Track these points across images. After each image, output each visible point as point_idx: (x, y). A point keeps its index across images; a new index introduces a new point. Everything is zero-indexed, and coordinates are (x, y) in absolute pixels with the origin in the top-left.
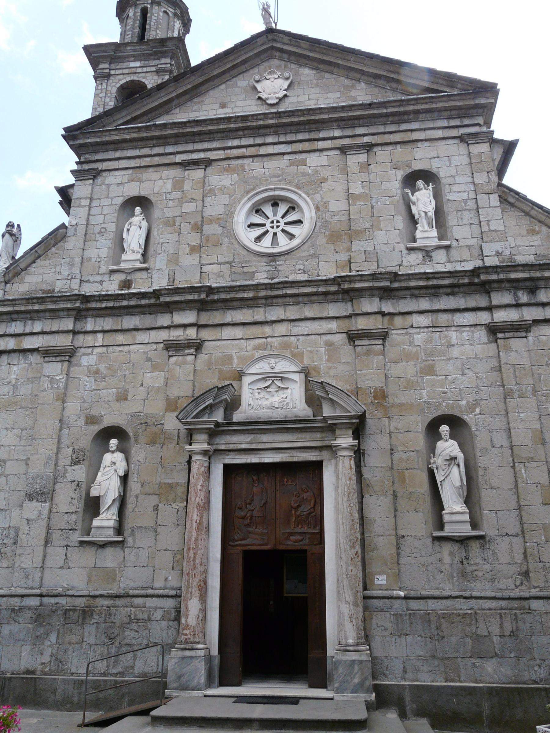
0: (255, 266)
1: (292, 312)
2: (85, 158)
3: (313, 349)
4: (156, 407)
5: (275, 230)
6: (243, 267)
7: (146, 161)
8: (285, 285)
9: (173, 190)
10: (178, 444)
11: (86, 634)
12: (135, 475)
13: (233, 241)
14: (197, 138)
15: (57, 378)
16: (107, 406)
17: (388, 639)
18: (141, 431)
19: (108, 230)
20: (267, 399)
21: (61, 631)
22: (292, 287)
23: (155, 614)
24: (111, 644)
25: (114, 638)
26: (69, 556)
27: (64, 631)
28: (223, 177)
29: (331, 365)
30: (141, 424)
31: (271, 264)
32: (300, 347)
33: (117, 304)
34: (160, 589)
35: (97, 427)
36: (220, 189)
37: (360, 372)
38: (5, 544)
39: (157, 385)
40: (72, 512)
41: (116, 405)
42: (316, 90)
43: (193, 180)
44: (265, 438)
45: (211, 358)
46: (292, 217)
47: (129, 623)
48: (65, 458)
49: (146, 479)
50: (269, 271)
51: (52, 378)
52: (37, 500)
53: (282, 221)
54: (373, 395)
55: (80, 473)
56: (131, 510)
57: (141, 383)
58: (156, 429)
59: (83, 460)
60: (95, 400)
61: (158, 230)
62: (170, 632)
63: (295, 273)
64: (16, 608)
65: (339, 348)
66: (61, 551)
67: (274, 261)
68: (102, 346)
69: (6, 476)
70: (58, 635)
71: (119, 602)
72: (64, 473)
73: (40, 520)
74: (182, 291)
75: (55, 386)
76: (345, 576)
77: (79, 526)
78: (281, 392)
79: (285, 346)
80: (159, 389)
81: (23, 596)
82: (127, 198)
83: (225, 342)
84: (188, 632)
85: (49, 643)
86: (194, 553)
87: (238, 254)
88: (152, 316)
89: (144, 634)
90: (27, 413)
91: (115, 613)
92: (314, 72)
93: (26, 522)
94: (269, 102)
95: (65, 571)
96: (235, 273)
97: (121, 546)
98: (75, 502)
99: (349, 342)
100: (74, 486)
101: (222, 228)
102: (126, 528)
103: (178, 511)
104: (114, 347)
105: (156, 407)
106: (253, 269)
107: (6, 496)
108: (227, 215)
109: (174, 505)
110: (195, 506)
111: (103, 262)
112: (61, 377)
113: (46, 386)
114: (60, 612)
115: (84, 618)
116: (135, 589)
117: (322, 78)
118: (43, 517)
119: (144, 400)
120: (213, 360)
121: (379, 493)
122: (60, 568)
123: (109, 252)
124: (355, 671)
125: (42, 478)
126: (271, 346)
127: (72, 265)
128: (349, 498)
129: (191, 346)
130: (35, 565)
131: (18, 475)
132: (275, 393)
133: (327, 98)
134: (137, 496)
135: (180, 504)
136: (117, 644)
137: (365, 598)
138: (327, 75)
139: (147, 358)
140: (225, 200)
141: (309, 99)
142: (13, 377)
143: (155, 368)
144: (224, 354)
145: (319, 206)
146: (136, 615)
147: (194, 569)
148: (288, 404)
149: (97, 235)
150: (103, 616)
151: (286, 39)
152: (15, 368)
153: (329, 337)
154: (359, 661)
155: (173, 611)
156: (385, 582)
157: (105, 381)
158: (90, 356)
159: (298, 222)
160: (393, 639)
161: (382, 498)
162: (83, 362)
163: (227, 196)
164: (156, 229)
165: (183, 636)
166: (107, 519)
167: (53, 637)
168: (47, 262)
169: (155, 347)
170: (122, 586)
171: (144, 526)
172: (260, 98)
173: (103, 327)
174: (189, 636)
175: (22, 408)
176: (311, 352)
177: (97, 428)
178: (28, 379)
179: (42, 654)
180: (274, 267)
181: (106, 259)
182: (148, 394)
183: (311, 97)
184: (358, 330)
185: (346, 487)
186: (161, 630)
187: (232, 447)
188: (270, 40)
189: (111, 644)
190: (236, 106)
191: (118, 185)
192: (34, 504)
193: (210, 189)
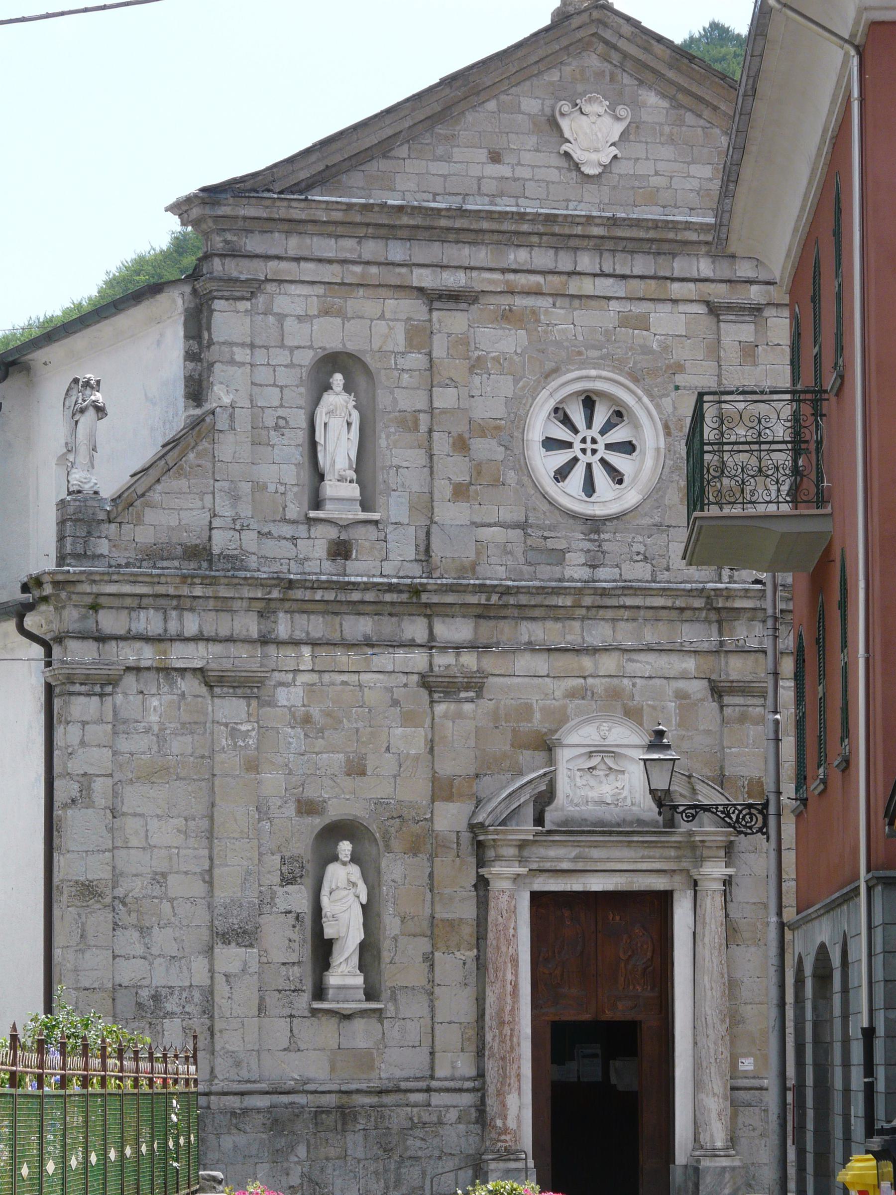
0: (566, 537)
1: (625, 634)
2: (226, 242)
3: (657, 703)
4: (415, 790)
5: (578, 446)
6: (546, 538)
7: (354, 273)
8: (626, 592)
9: (408, 350)
10: (458, 856)
11: (350, 1145)
12: (390, 904)
13: (525, 479)
14: (452, 237)
15: (243, 728)
16: (331, 782)
17: (757, 1141)
18: (392, 830)
19: (292, 424)
20: (592, 788)
21: (312, 1141)
22: (635, 595)
23: (448, 1115)
24: (389, 1158)
25: (392, 1149)
26: (295, 1031)
27: (316, 1142)
28: (500, 332)
29: (684, 733)
30: (393, 818)
31: (592, 536)
32: (637, 698)
33: (342, 597)
34: (446, 1079)
35: (318, 820)
36: (496, 360)
37: (728, 751)
38: (188, 1013)
39: (413, 752)
40: (294, 963)
41: (347, 783)
42: (667, 152)
43: (449, 335)
44: (595, 853)
45: (498, 708)
46: (618, 435)
47: (411, 1129)
48: (269, 872)
49: (407, 911)
50: (589, 551)
51: (233, 729)
52: (238, 944)
53: (602, 441)
54: (746, 790)
55: (298, 898)
56: (388, 960)
57: (385, 745)
58: (416, 829)
59: (301, 877)
60: (309, 772)
61: (388, 437)
62: (471, 1139)
63: (631, 559)
64: (238, 1111)
65: (696, 705)
66: (284, 1024)
67: (597, 531)
68: (312, 670)
69: (171, 901)
70: (308, 1147)
71: (388, 1099)
72: (272, 898)
73: (248, 976)
74: (462, 588)
75: (241, 743)
76: (712, 1060)
77: (308, 985)
78: (612, 777)
79: (615, 694)
80: (417, 758)
81: (242, 1094)
82: (321, 353)
83: (519, 680)
84: (507, 1138)
85: (296, 1159)
86: (511, 1030)
87: (534, 509)
88: (394, 619)
89: (434, 1142)
90: (190, 789)
91: (390, 1116)
92: (665, 104)
93: (224, 978)
94: (586, 170)
95: (292, 1055)
96: (532, 549)
97: (377, 1015)
98: (296, 946)
99: (712, 696)
100: (291, 919)
101: (503, 449)
102: (383, 988)
103: (464, 964)
104: (331, 674)
105: (415, 790)
106: (561, 545)
107: (177, 935)
108: (512, 422)
109: (458, 954)
110: (508, 960)
111: (290, 496)
112: (250, 728)
113: (224, 742)
114: (306, 1116)
115: (344, 1124)
116: (407, 1079)
117: (680, 122)
118: (251, 970)
119: (395, 777)
120: (502, 712)
121: (749, 943)
122: (285, 1050)
123: (298, 474)
124: (726, 1180)
125: (241, 906)
126: (593, 693)
127: (235, 498)
128: (720, 952)
129: (471, 687)
130: (249, 1047)
131: (192, 900)
132: (603, 779)
133: (689, 176)
134: (395, 938)
135: (468, 953)
136: (396, 1158)
137: (733, 1089)
138: (689, 118)
139: (392, 699)
140: (505, 386)
141: (657, 173)
142: (154, 718)
143: (408, 719)
144: (519, 702)
145: (670, 424)
146: (420, 1117)
147: (512, 1051)
148: (625, 798)
149: (272, 433)
150: (373, 1119)
151: (627, 29)
152: (155, 702)
153: (681, 684)
154: (730, 1167)
155: (473, 1110)
156: (752, 1068)
157: (323, 738)
158: (292, 689)
159: (628, 448)
160: (763, 1142)
161: (753, 949)
162: (280, 699)
163: (510, 378)
164: (383, 436)
165: (500, 1144)
166: (344, 973)
167: (302, 1151)
168: (183, 483)
169: (405, 681)
170: (383, 1075)
171: (410, 985)
172: (567, 155)
173: (308, 633)
174: (510, 1144)
175: (179, 778)
176: (654, 708)
177: (318, 823)
178: (183, 724)
179: (288, 1174)
180: (597, 544)
181: (295, 489)
182: (400, 766)
183: (661, 166)
184: (732, 682)
185: (716, 937)
186: (459, 1136)
187: (548, 866)
188: (593, 21)
189: (389, 1158)
190: (519, 164)
191: (300, 318)
192: (234, 951)
193: (479, 358)
